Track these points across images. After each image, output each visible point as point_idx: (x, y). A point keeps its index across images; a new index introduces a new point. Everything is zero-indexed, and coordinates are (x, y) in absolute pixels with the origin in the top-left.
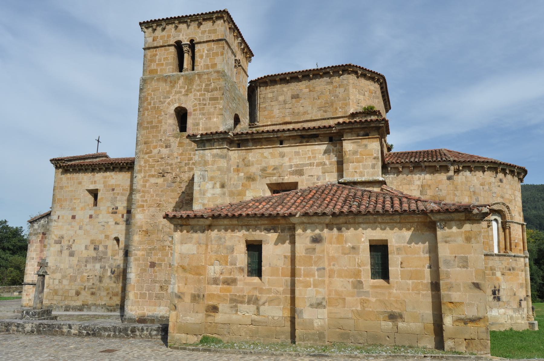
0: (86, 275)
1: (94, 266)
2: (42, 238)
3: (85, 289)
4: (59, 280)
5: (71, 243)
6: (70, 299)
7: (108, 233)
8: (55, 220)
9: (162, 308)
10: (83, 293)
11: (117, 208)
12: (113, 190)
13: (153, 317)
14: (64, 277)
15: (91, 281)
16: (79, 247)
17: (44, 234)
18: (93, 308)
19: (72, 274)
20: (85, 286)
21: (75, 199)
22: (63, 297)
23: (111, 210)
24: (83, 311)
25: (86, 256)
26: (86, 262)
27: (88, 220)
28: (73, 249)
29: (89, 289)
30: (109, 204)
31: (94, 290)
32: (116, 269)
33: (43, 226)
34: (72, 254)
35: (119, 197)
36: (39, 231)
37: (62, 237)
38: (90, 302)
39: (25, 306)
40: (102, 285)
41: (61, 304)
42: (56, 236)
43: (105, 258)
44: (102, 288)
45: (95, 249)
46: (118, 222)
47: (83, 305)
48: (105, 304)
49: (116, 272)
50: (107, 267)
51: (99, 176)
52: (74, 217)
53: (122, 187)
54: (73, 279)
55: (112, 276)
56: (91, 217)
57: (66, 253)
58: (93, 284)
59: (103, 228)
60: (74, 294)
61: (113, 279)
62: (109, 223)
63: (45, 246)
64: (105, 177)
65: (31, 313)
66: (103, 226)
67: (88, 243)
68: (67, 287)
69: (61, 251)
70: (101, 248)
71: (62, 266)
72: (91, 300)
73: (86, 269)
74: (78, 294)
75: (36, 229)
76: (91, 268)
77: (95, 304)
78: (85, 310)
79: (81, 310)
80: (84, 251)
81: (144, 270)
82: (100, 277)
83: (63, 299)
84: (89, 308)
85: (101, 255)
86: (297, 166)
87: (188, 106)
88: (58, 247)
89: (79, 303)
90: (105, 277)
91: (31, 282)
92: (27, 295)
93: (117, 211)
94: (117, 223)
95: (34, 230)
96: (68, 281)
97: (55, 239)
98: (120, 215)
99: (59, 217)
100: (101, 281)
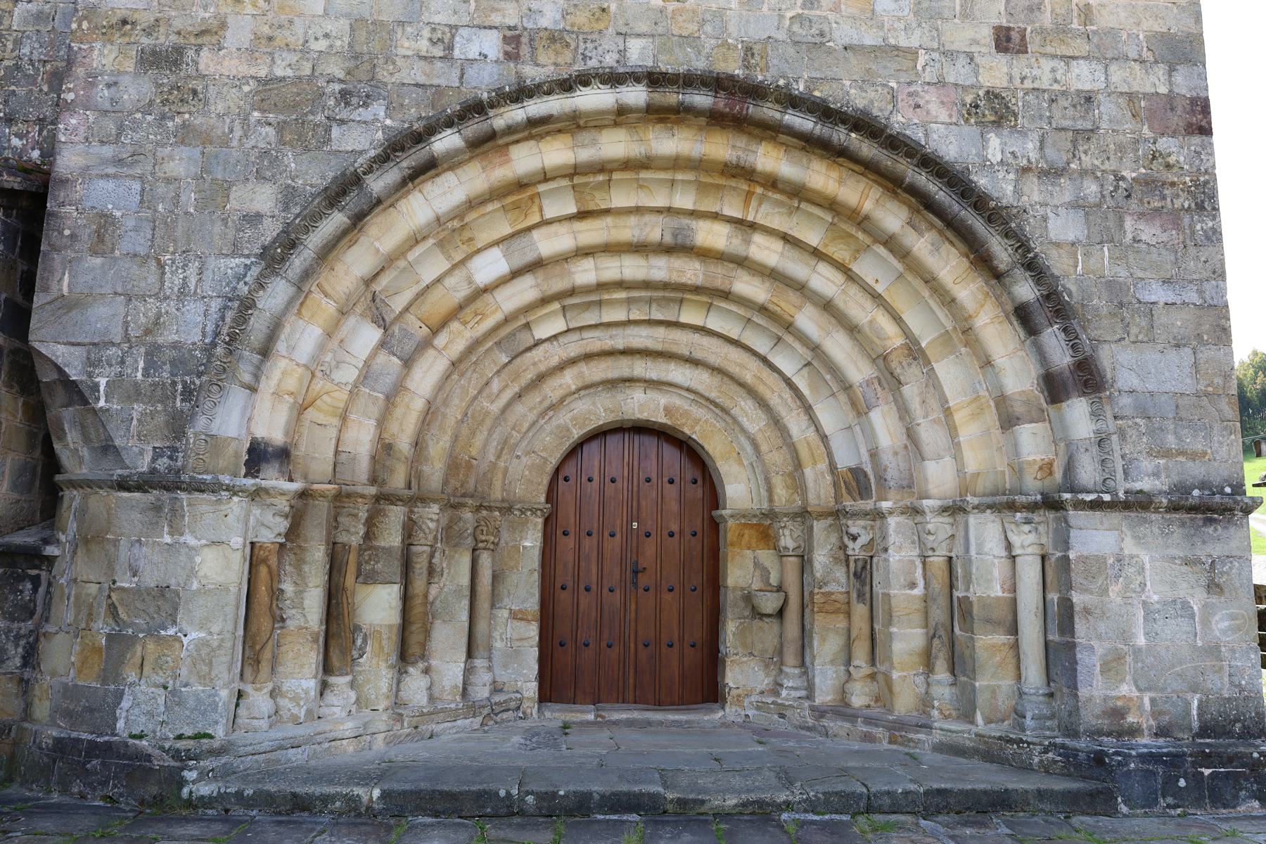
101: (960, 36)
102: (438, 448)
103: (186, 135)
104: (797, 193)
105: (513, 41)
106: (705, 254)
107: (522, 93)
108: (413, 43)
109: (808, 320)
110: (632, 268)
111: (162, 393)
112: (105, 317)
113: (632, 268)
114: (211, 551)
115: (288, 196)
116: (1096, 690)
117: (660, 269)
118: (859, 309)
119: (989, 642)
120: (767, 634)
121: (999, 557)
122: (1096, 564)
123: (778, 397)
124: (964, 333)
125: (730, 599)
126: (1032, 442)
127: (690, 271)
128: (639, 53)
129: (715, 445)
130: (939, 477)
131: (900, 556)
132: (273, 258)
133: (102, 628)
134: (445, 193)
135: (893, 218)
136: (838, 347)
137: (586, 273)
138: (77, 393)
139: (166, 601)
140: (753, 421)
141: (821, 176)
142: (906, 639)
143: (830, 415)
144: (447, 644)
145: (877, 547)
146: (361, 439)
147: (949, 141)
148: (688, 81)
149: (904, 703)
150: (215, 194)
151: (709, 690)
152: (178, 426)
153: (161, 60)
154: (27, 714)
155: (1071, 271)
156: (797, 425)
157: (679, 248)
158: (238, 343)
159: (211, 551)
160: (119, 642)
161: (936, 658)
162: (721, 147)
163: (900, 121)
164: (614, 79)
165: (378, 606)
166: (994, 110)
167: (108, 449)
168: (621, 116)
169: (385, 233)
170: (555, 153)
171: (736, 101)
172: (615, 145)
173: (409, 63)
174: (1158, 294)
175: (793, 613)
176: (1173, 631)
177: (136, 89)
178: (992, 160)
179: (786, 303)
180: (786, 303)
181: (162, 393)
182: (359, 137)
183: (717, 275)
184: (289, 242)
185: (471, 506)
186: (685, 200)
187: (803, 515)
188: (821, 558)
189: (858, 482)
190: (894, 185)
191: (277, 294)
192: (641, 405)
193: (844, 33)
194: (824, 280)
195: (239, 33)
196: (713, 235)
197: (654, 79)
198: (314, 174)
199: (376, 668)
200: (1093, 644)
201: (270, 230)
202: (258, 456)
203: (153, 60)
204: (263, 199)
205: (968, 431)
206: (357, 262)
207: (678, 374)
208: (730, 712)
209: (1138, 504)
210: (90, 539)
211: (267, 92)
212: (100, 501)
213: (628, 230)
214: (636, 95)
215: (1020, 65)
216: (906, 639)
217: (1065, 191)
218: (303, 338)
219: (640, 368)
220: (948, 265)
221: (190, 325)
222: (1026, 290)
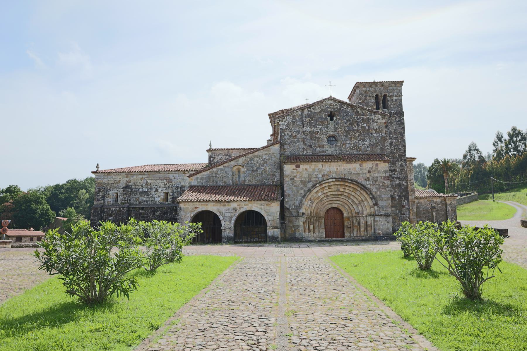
101: (364, 172)
102: (315, 212)
103: (295, 186)
104: (350, 187)
105: (323, 175)
106: (341, 191)
107: (324, 181)
108: (314, 176)
109: (352, 197)
110: (334, 193)
111: (296, 209)
112: (290, 203)
113: (334, 193)
114: (301, 222)
115: (304, 191)
116: (377, 231)
117: (336, 193)
118: (357, 197)
119: (369, 228)
120: (349, 230)
121: (370, 220)
122: (377, 221)
123: (349, 205)
124: (366, 200)
125: (345, 226)
126: (372, 210)
127: (339, 193)
128: (334, 176)
129: (343, 210)
130: (365, 213)
131: (362, 221)
132: (304, 197)
133: (293, 229)
134: (317, 189)
135: (359, 189)
136: (355, 200)
137: (329, 194)
138: (289, 209)
139: (298, 226)
140: (347, 207)
141: (352, 185)
142: (362, 229)
143: (355, 206)
144: (317, 230)
145: (360, 220)
146: (309, 211)
147: (363, 182)
148: (339, 178)
149: (362, 235)
150: (298, 191)
151: (344, 236)
152: (298, 212)
153: (293, 179)
154: (285, 236)
155: (375, 194)
156: (351, 207)
157: (338, 191)
158: (300, 205)
159: (301, 222)
160: (295, 230)
161: (364, 230)
162: (342, 183)
163: (359, 181)
164: (332, 179)
165: (311, 227)
166: (368, 179)
167: (292, 214)
168: (333, 181)
169: (312, 193)
170: (327, 185)
171: (343, 180)
172: (332, 183)
173: (314, 178)
174: (383, 196)
175: (351, 228)
176: (384, 226)
177: (290, 182)
178: (368, 184)
179: (349, 196)
180: (349, 196)
181: (296, 209)
182: (310, 185)
183: (342, 193)
184: (305, 195)
185: (318, 217)
186: (339, 187)
187: (352, 217)
188: (354, 221)
189: (358, 213)
190: (359, 186)
191: (304, 199)
192: (334, 205)
193: (353, 172)
194: (353, 194)
195: (298, 176)
196: (342, 190)
197: (336, 178)
198: (306, 189)
199: (312, 232)
200: (377, 228)
201: (303, 194)
202: (303, 214)
203: (291, 179)
204: (302, 191)
205: (368, 208)
206: (310, 196)
207: (338, 202)
208: (346, 238)
209: (381, 215)
210: (290, 221)
211: (301, 182)
212: (290, 218)
213: (333, 190)
214: (334, 180)
215: (370, 174)
216: (362, 229)
217: (375, 186)
218: (306, 203)
219: (334, 202)
220: (364, 193)
221: (297, 203)
222: (371, 196)
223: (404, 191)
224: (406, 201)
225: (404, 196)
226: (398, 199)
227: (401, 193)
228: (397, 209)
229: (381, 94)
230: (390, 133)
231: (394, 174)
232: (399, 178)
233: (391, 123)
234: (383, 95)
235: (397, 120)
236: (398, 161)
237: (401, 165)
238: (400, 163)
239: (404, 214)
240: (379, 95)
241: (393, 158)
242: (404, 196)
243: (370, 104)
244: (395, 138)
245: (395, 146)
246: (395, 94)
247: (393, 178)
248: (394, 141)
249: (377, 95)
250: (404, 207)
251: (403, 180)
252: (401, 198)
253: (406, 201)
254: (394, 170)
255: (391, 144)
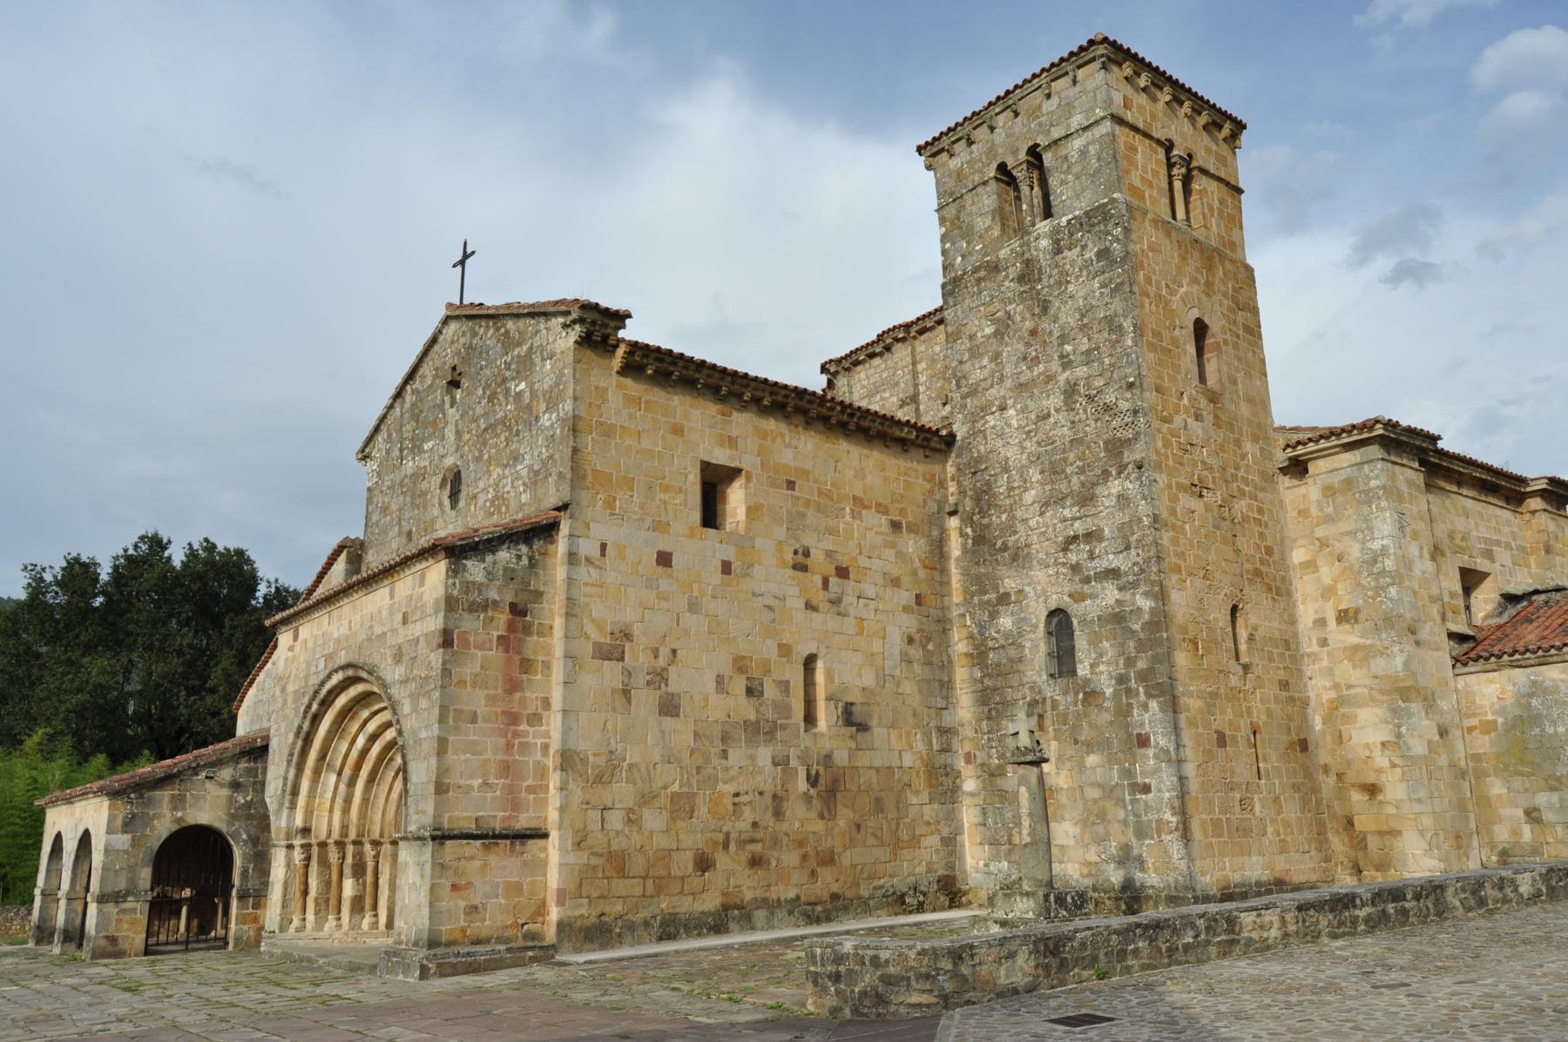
0: (730, 788)
1: (752, 758)
2: (511, 627)
3: (726, 845)
4: (631, 810)
5: (662, 662)
6: (676, 888)
7: (787, 638)
8: (588, 559)
9: (1254, 858)
10: (722, 861)
11: (807, 554)
12: (791, 485)
13: (1243, 885)
14: (646, 799)
15: (748, 815)
16: (695, 678)
17: (517, 610)
18: (760, 915)
19: (676, 788)
20: (727, 835)
21: (665, 489)
22: (650, 882)
23: (789, 557)
24: (727, 931)
25: (722, 716)
26: (725, 738)
27: (716, 578)
28: (674, 686)
29: (742, 843)
30: (780, 532)
31: (758, 847)
32: (821, 769)
33: (510, 575)
34: (669, 707)
35: (812, 517)
36: (493, 594)
37: (628, 636)
38: (748, 895)
39: (449, 944)
40: (784, 827)
41: (644, 914)
42: (600, 628)
43: (783, 727)
44: (785, 840)
45: (750, 692)
46: (814, 602)
47: (726, 908)
48: (798, 898)
49: (822, 781)
50: (793, 763)
51: (743, 422)
52: (664, 559)
53: (816, 481)
54: (682, 806)
55: (813, 792)
56: (726, 568)
57: (646, 699)
58: (755, 825)
59: (770, 615)
60: (691, 865)
61: (817, 804)
62: (790, 603)
63: (526, 665)
64: (764, 435)
65: (1069, 899)
66: (770, 608)
67: (727, 669)
68: (661, 841)
69: (626, 693)
70: (770, 691)
71: (633, 755)
72: (749, 887)
73: (727, 769)
74: (704, 864)
75: (480, 587)
76: (744, 763)
77: (765, 900)
78: (733, 926)
79: (719, 929)
80: (714, 699)
81: (1208, 753)
82: (775, 797)
83: (650, 889)
84: (747, 921)
85: (770, 715)
86: (1486, 540)
87: (1215, 325)
88: (611, 673)
89: (710, 903)
90: (792, 797)
91: (471, 827)
92: (455, 887)
93: (808, 562)
94: (810, 607)
95: (468, 586)
96: (666, 815)
97: (595, 636)
98: (818, 580)
99: (603, 547)
100: (778, 814)
223: (1141, 647)
224: (1154, 705)
225: (1143, 677)
226: (1116, 695)
227: (1130, 662)
228: (1111, 760)
229: (1015, 152)
230: (1063, 339)
231: (1092, 557)
232: (1112, 573)
233: (1063, 281)
234: (1022, 156)
235: (1090, 254)
236: (1106, 474)
237: (1123, 499)
238: (1115, 486)
239: (1146, 789)
240: (1010, 163)
241: (1082, 471)
242: (1143, 677)
243: (981, 223)
244: (1089, 357)
245: (1090, 398)
246: (1077, 120)
247: (1087, 580)
248: (1082, 371)
249: (1002, 168)
250: (1143, 741)
251: (1134, 585)
252: (1128, 691)
253: (1154, 705)
254: (1089, 536)
255: (1070, 391)
